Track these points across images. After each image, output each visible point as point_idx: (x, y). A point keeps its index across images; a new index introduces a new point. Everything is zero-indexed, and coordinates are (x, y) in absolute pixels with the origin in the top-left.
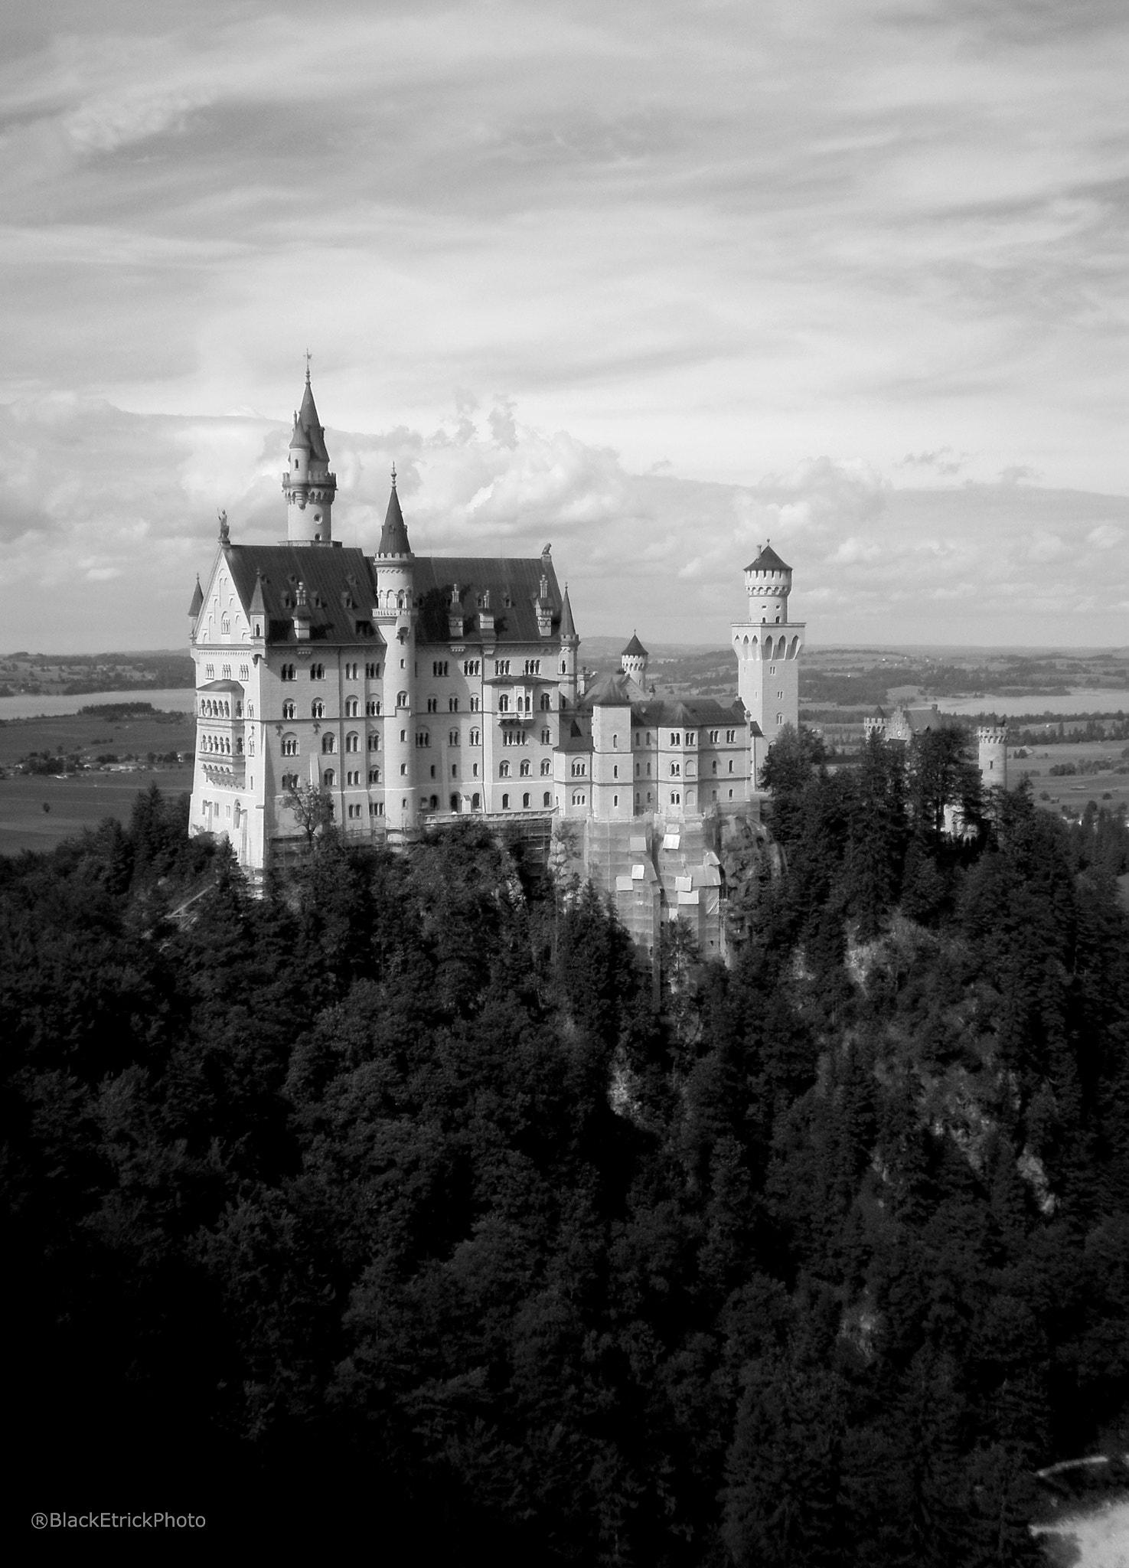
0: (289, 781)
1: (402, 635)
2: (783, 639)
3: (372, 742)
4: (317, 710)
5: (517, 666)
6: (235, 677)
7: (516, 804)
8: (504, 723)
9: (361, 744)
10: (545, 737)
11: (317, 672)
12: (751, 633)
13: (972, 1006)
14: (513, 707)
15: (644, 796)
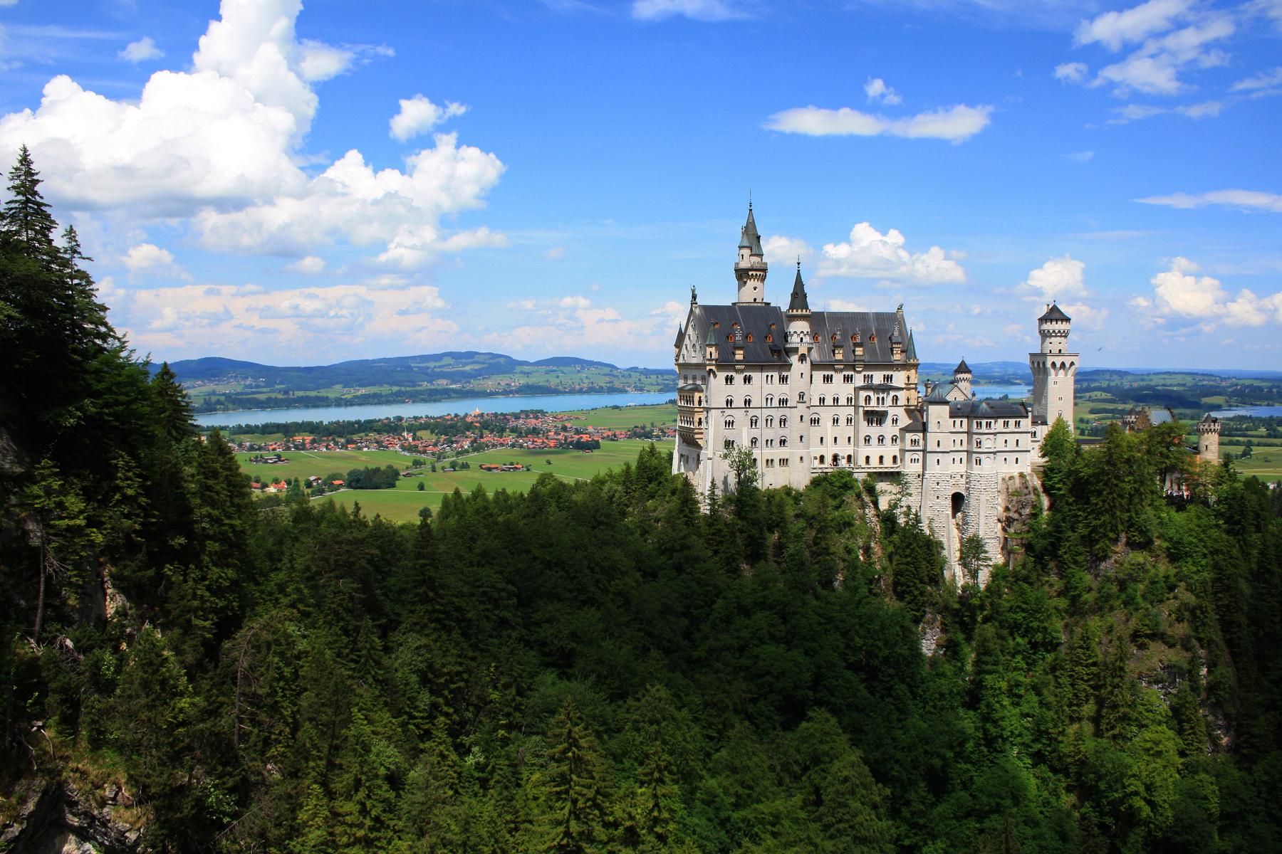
0: (729, 444)
1: (802, 358)
2: (1063, 365)
3: (783, 421)
4: (748, 402)
5: (878, 377)
6: (699, 382)
7: (874, 462)
8: (867, 413)
9: (776, 423)
10: (895, 421)
11: (748, 380)
12: (1041, 359)
13: (1173, 604)
14: (873, 402)
15: (957, 460)
